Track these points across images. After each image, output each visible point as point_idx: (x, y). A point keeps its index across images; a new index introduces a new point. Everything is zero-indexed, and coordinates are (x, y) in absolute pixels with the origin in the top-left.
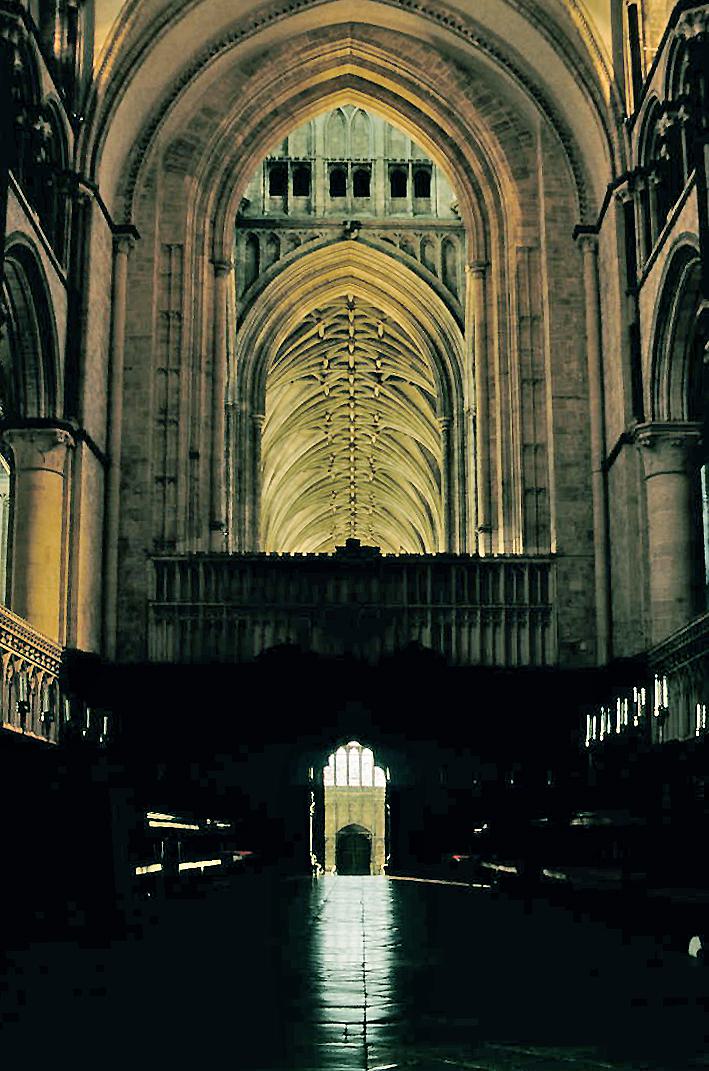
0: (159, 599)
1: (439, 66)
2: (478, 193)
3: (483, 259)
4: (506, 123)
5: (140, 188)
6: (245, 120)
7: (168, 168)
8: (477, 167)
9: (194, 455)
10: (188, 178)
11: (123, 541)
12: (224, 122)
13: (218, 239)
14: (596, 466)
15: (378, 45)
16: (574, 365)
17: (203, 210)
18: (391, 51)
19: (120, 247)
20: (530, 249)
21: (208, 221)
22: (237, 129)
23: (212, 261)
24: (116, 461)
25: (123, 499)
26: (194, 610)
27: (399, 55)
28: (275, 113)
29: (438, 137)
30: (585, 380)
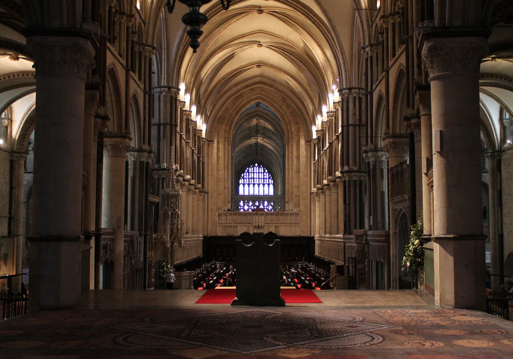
0: (219, 220)
1: (279, 97)
2: (287, 125)
3: (288, 141)
4: (293, 111)
5: (213, 130)
6: (235, 109)
7: (218, 123)
8: (287, 120)
9: (225, 188)
10: (223, 126)
11: (211, 209)
12: (231, 111)
13: (229, 137)
14: (309, 193)
15: (265, 92)
16: (305, 171)
17: (226, 131)
18: (268, 93)
19: (210, 144)
20: (297, 141)
21: (227, 134)
22: (233, 111)
23: (228, 142)
24: (210, 192)
25: (211, 200)
26: (226, 223)
27: (270, 94)
28: (242, 106)
29: (279, 112)
30: (307, 174)
